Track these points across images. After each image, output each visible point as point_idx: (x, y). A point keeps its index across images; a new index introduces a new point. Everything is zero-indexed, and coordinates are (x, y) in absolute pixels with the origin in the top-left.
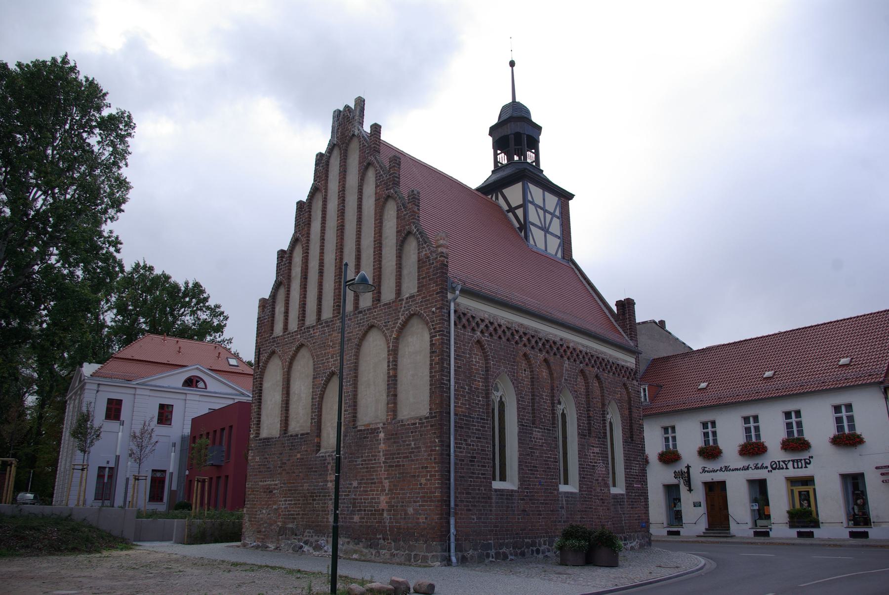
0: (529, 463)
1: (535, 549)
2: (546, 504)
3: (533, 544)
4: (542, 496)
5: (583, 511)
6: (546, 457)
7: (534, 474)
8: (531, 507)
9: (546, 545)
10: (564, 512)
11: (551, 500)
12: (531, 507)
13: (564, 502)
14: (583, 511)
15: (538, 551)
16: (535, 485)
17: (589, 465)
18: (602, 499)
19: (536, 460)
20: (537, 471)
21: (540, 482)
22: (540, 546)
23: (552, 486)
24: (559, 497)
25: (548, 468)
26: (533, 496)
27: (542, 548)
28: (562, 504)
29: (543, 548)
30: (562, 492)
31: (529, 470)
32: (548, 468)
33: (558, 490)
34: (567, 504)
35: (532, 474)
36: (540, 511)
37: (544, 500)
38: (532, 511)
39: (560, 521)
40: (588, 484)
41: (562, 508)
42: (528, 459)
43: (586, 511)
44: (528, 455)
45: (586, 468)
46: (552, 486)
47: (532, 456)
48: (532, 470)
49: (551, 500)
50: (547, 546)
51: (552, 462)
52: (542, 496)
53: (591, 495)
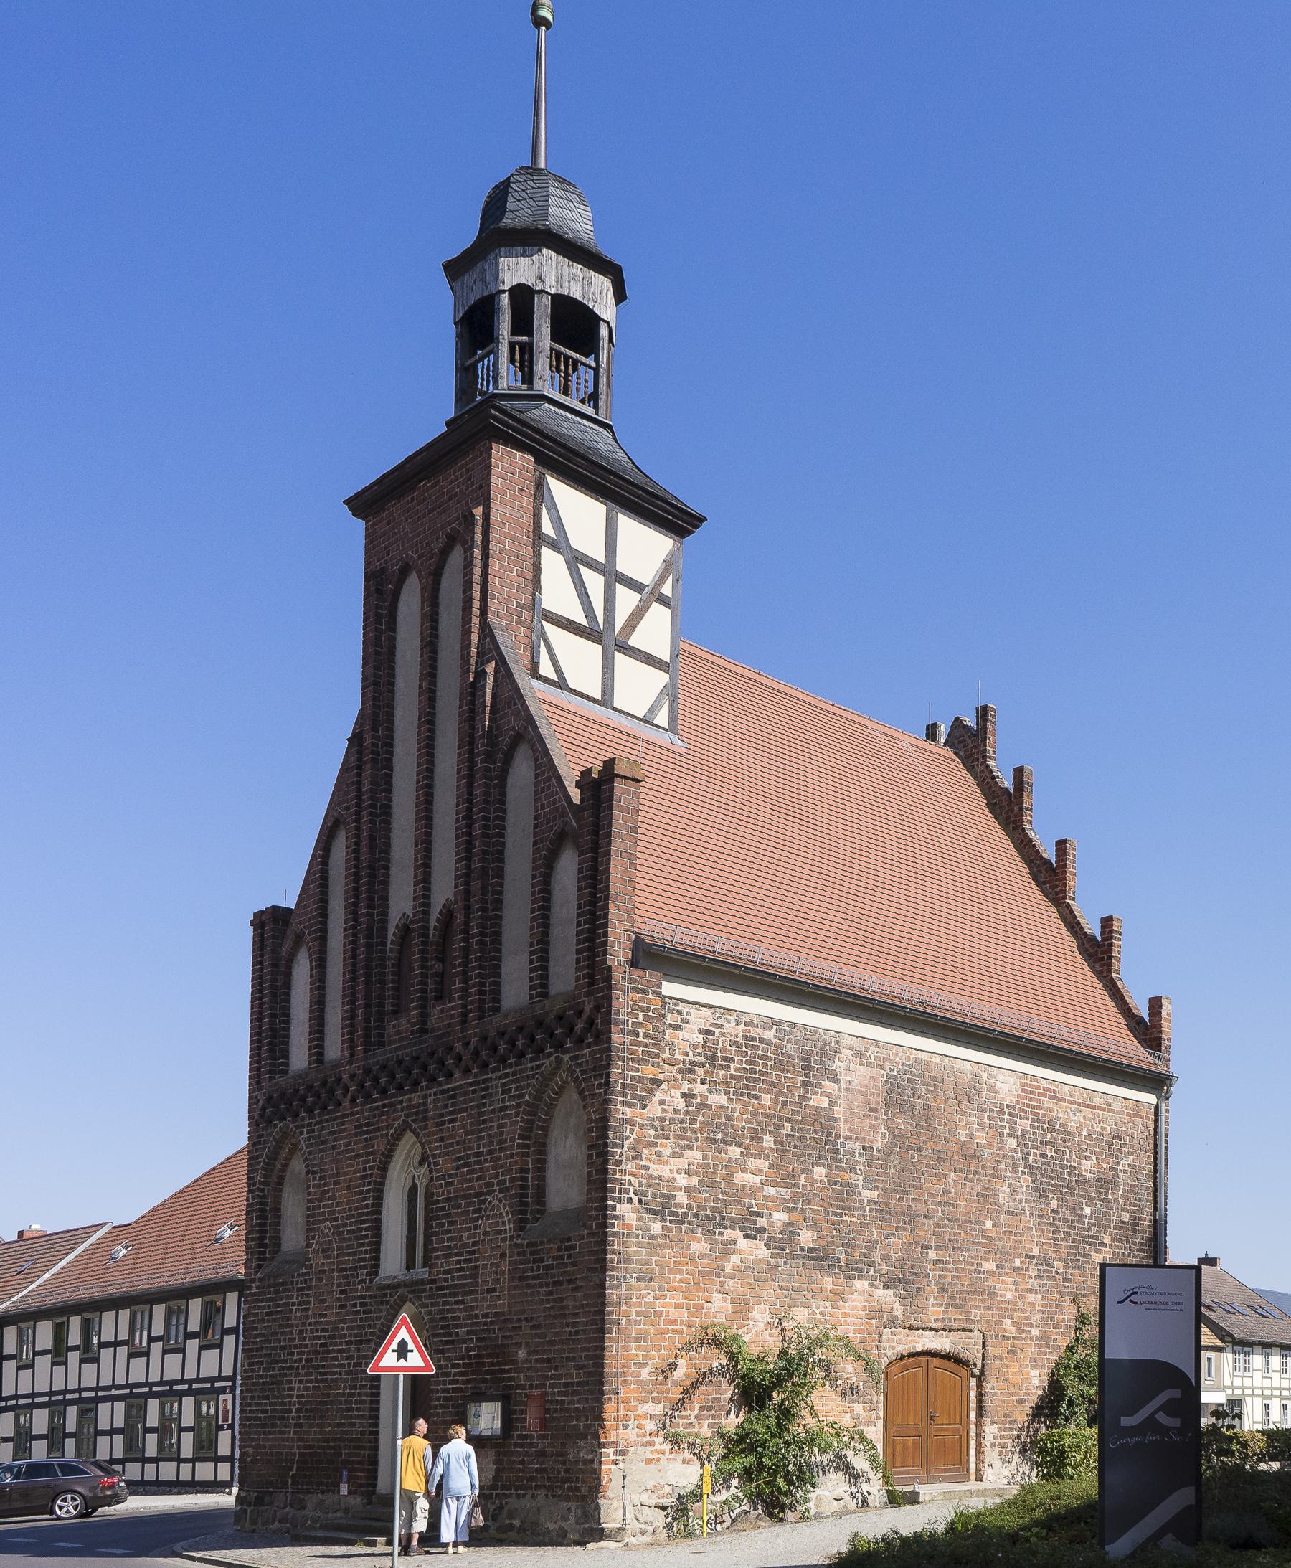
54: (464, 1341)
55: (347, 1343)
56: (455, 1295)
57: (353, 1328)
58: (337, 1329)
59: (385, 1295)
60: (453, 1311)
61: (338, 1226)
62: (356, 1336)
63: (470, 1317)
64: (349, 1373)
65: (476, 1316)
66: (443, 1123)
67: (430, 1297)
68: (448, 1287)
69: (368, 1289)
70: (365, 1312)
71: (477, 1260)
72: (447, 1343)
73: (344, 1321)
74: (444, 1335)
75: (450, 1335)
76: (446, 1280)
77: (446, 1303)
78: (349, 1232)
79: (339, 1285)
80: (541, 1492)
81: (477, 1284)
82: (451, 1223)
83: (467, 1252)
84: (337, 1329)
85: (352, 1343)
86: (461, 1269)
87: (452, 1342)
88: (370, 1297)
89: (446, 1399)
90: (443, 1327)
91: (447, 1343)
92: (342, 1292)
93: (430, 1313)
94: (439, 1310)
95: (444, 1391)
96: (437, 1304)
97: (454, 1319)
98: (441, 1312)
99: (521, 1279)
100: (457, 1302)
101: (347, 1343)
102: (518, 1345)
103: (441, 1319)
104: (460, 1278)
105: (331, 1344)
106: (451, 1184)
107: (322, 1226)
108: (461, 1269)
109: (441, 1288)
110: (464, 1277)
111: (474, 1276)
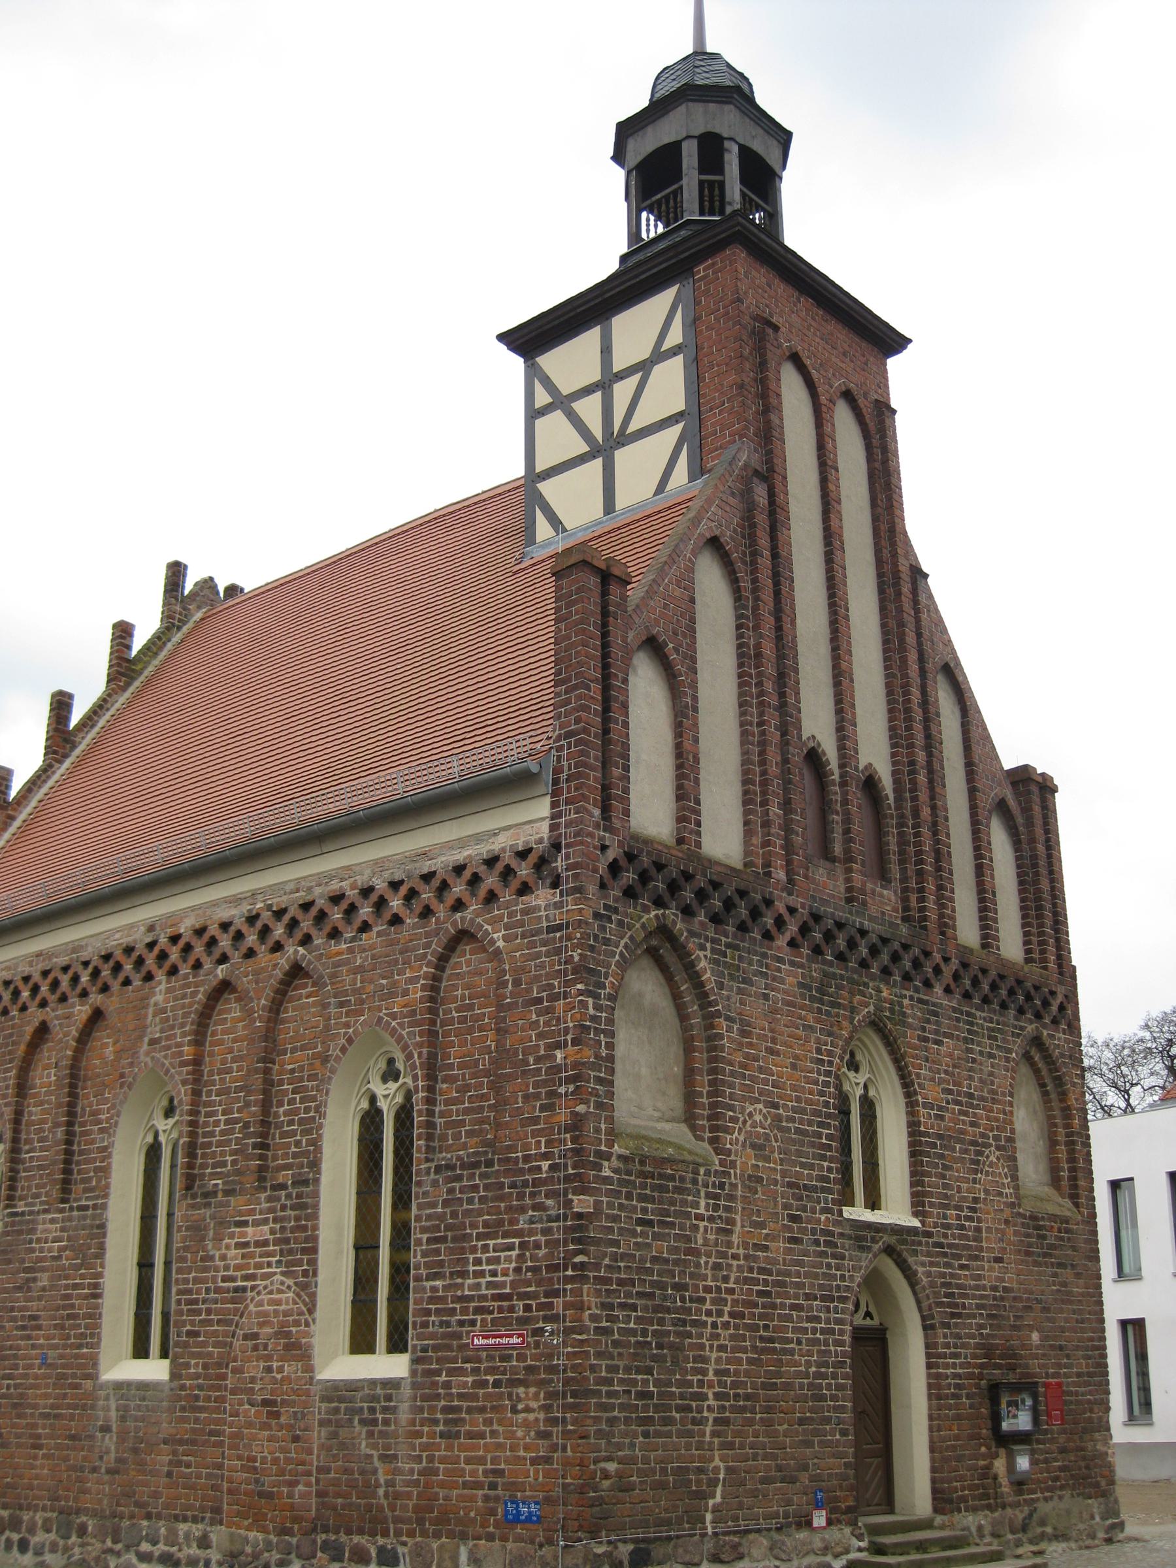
0: (21, 1309)
1: (15, 1537)
2: (56, 1416)
3: (15, 1524)
4: (46, 1396)
5: (181, 1442)
6: (67, 1287)
7: (29, 1337)
8: (14, 1426)
9: (48, 1531)
10: (110, 1442)
11: (69, 1406)
12: (14, 1426)
13: (113, 1414)
14: (181, 1442)
15: (23, 1546)
16: (31, 1367)
17: (218, 1290)
18: (265, 1403)
19: (40, 1298)
20: (39, 1328)
21: (44, 1357)
22: (32, 1530)
23: (79, 1367)
24: (97, 1399)
25: (70, 1317)
26: (21, 1396)
27: (35, 1540)
28: (107, 1419)
29: (39, 1538)
30: (108, 1382)
31: (17, 1328)
32: (70, 1317)
33: (97, 1378)
34: (123, 1419)
35: (22, 1338)
36: (39, 1437)
37: (52, 1407)
38: (18, 1436)
39: (94, 1470)
40: (210, 1355)
41: (106, 1429)
42: (17, 1300)
43: (193, 1442)
44: (19, 1289)
45: (205, 1301)
46: (79, 1367)
47: (29, 1289)
48: (24, 1328)
49: (69, 1406)
50: (52, 1536)
51: (86, 1297)
52: (46, 1396)
53: (218, 1388)
54: (974, 1316)
55: (808, 1297)
56: (959, 1257)
57: (816, 1276)
58: (788, 1274)
59: (864, 1239)
60: (959, 1277)
61: (778, 1118)
62: (821, 1287)
63: (977, 1288)
64: (814, 1342)
65: (984, 1288)
66: (926, 1040)
67: (928, 1254)
68: (950, 1246)
69: (837, 1223)
70: (834, 1256)
71: (979, 1220)
72: (953, 1315)
73: (801, 1264)
74: (949, 1305)
75: (956, 1306)
76: (945, 1236)
77: (947, 1265)
78: (798, 1131)
79: (786, 1206)
80: (1067, 1493)
81: (981, 1249)
82: (945, 1167)
83: (968, 1207)
84: (788, 1274)
85: (816, 1299)
86: (962, 1227)
87: (959, 1315)
88: (841, 1235)
89: (957, 1386)
90: (947, 1295)
91: (953, 1315)
92: (794, 1219)
93: (929, 1274)
94: (940, 1272)
95: (956, 1376)
96: (937, 1265)
97: (959, 1286)
98: (943, 1275)
99: (1028, 1253)
100: (962, 1267)
101: (808, 1297)
102: (1031, 1328)
103: (944, 1285)
104: (961, 1237)
105: (779, 1295)
106: (942, 1118)
107: (750, 1109)
108: (962, 1227)
109: (941, 1245)
110: (966, 1238)
111: (978, 1239)
